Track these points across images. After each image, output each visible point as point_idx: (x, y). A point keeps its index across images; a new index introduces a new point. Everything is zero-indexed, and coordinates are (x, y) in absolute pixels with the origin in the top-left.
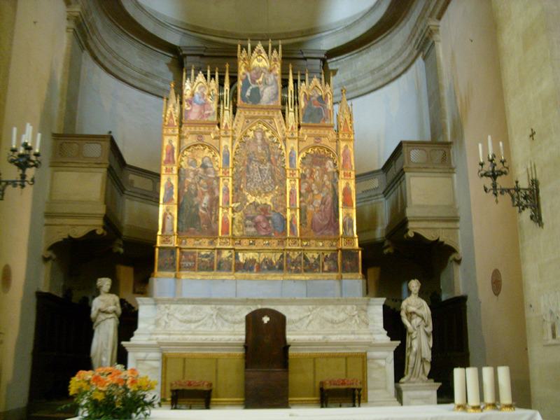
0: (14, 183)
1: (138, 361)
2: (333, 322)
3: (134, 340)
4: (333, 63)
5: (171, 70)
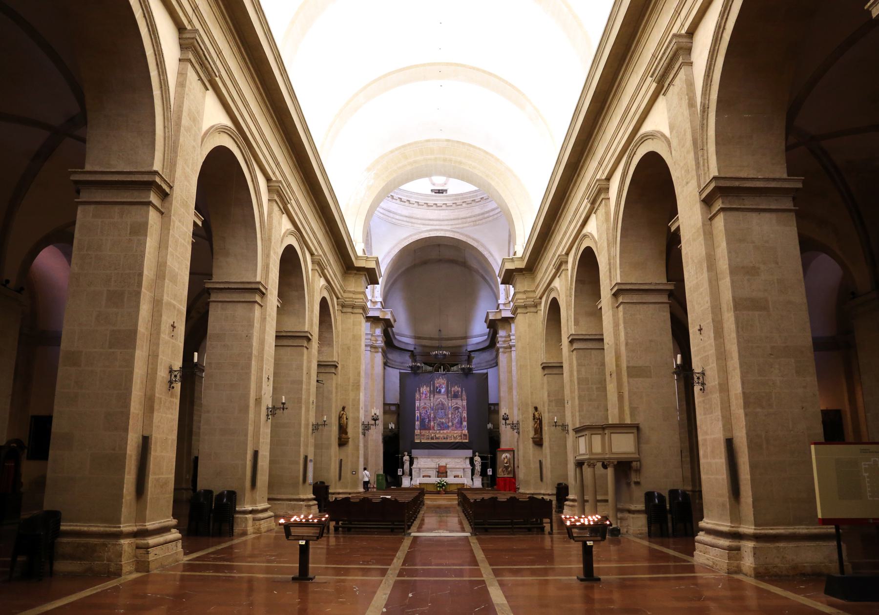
3: (413, 466)
4: (473, 355)
5: (411, 358)
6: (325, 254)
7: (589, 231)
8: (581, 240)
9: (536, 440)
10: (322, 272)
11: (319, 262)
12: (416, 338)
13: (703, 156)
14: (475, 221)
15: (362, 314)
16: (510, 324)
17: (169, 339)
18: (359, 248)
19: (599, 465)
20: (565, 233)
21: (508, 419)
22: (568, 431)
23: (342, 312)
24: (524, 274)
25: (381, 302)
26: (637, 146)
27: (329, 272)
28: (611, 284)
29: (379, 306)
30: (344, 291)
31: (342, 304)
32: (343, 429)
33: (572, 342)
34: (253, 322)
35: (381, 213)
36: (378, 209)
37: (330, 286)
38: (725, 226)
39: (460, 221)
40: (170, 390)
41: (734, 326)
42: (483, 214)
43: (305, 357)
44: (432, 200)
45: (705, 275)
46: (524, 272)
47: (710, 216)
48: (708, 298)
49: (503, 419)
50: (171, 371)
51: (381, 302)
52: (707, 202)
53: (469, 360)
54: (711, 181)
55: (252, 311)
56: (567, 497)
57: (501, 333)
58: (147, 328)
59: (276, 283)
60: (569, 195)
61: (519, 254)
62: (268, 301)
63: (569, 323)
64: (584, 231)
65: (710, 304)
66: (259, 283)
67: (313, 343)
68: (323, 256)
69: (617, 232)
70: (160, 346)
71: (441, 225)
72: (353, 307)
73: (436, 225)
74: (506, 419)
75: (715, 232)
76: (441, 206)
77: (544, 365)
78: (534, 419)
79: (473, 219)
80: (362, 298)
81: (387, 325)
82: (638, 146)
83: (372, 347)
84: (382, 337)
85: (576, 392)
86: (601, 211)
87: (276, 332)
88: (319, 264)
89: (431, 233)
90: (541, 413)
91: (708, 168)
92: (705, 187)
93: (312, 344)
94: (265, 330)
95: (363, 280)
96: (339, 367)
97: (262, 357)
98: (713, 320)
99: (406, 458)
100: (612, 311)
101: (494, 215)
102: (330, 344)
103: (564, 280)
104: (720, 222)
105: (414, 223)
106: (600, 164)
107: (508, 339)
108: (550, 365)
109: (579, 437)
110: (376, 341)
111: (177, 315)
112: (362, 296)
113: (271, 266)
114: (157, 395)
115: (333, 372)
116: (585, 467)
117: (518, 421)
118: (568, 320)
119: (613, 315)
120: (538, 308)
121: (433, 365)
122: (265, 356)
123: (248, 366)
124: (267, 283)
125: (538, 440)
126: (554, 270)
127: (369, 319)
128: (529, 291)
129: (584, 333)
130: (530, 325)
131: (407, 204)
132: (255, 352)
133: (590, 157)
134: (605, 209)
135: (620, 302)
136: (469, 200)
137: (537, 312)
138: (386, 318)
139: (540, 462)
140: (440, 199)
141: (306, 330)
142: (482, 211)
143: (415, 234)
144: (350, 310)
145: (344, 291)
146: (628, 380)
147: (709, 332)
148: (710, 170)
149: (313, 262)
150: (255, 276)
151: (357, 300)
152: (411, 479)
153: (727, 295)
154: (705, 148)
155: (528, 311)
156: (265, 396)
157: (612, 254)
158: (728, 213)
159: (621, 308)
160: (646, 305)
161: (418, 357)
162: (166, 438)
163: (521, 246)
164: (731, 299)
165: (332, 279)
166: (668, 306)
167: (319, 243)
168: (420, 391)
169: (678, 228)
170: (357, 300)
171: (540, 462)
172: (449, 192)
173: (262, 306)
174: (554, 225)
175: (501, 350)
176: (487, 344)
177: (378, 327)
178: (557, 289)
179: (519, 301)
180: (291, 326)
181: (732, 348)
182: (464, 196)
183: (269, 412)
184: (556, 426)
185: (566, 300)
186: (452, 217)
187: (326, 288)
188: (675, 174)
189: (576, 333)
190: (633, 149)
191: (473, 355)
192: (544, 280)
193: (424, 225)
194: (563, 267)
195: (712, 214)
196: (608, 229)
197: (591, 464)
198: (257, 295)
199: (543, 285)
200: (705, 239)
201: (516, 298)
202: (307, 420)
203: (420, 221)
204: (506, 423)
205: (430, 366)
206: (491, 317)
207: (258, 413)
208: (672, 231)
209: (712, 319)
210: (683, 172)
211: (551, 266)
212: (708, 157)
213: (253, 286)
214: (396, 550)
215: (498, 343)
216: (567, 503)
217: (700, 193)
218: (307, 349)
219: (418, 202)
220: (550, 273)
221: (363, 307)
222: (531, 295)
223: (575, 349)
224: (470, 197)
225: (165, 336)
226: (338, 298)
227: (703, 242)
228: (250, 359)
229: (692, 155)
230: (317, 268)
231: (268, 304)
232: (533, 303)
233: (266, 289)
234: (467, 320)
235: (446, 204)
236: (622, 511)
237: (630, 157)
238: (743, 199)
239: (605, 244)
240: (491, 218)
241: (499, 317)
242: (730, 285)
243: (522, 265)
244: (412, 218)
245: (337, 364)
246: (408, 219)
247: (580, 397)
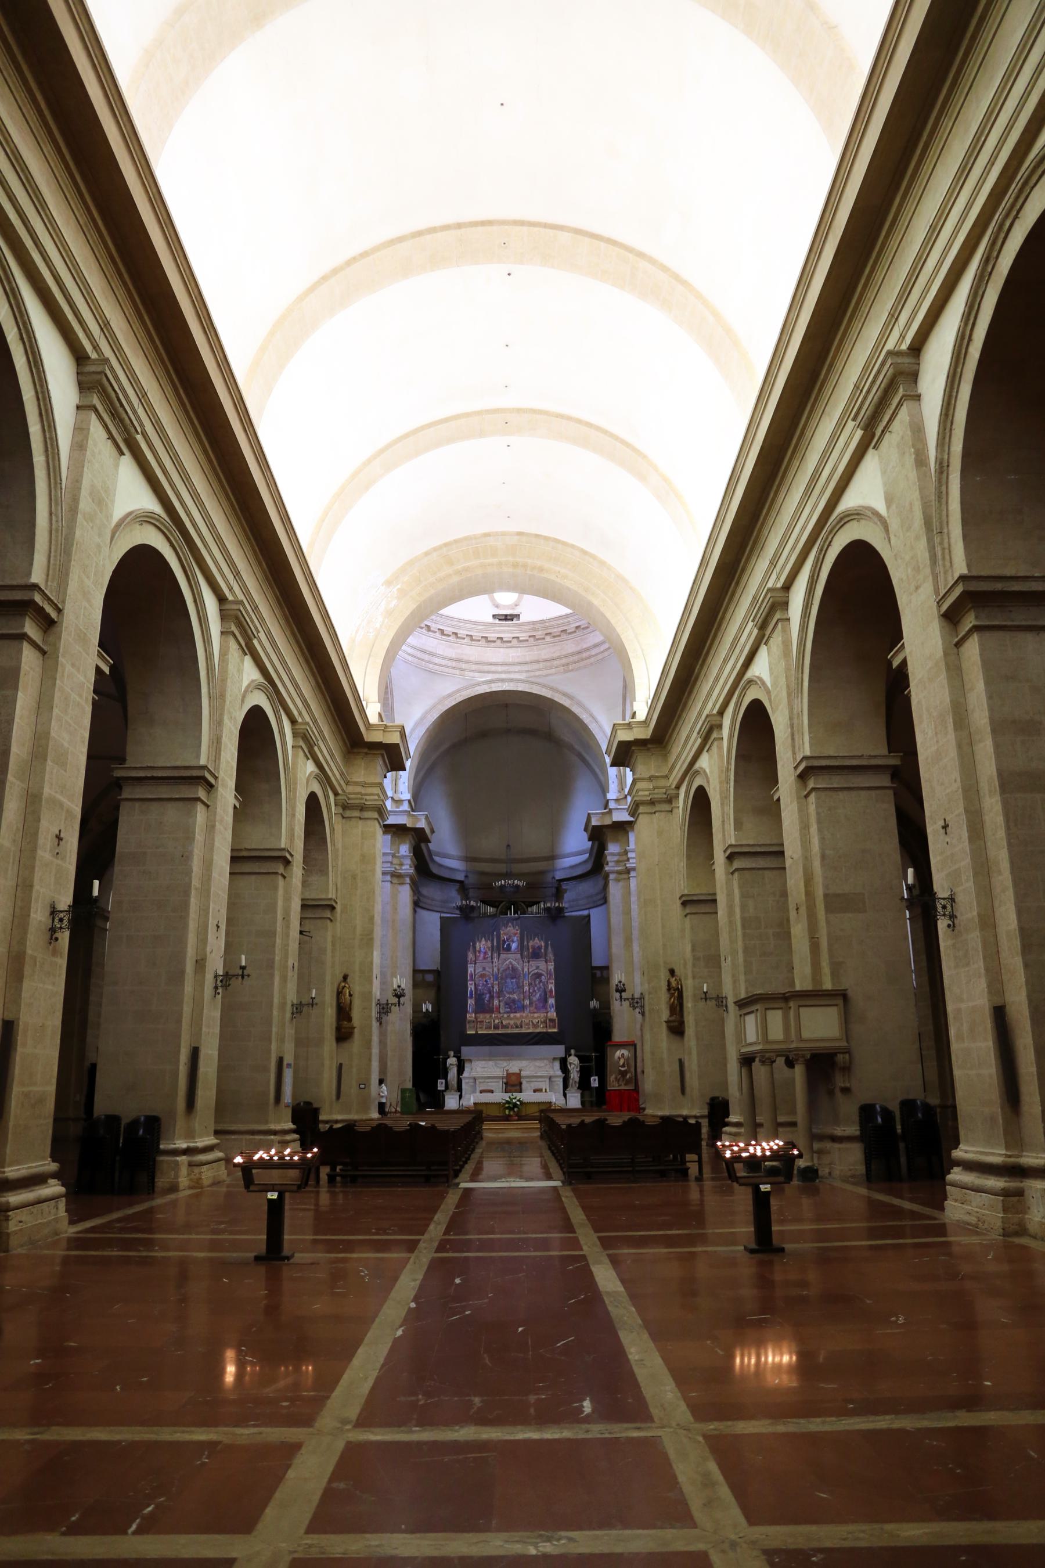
0: (395, 1005)
1: (466, 1083)
2: (539, 1067)
4: (564, 886)
6: (315, 721)
7: (757, 674)
8: (744, 688)
9: (672, 1024)
10: (309, 752)
11: (304, 734)
12: (468, 859)
13: (941, 543)
14: (567, 665)
15: (377, 819)
16: (627, 833)
17: (51, 858)
18: (373, 712)
19: (781, 1061)
20: (717, 679)
21: (624, 991)
22: (726, 1006)
23: (343, 818)
24: (648, 749)
25: (409, 801)
26: (834, 532)
27: (322, 752)
28: (794, 759)
29: (405, 807)
30: (347, 783)
31: (343, 804)
32: (343, 1012)
33: (730, 858)
34: (194, 833)
35: (409, 654)
36: (404, 647)
37: (323, 775)
38: (981, 655)
39: (541, 665)
40: (50, 943)
41: (1002, 818)
42: (579, 653)
43: (281, 892)
44: (495, 631)
45: (951, 736)
46: (649, 746)
47: (956, 640)
48: (956, 775)
49: (617, 991)
50: (54, 912)
51: (409, 801)
52: (951, 617)
53: (559, 894)
54: (956, 582)
55: (191, 814)
56: (726, 1120)
57: (613, 848)
58: (14, 841)
59: (232, 767)
60: (723, 618)
61: (641, 716)
62: (219, 797)
63: (726, 826)
64: (749, 675)
65: (960, 784)
66: (204, 767)
67: (294, 868)
68: (312, 725)
69: (802, 673)
70: (37, 869)
71: (509, 672)
72: (362, 808)
73: (501, 673)
74: (621, 990)
75: (964, 666)
76: (510, 642)
77: (684, 899)
78: (669, 989)
79: (564, 661)
80: (376, 792)
81: (419, 838)
82: (834, 531)
83: (395, 875)
84: (411, 859)
85: (740, 943)
86: (776, 640)
87: (232, 850)
88: (302, 736)
89: (493, 685)
90: (680, 980)
91: (951, 563)
92: (946, 593)
93: (292, 870)
94: (213, 844)
95: (379, 764)
96: (338, 907)
97: (208, 891)
98: (966, 811)
99: (452, 1061)
100: (798, 803)
101: (596, 655)
102: (324, 871)
103: (716, 756)
104: (973, 648)
105: (465, 670)
106: (773, 563)
107: (625, 858)
108: (695, 898)
109: (745, 1014)
110: (401, 864)
111: (66, 819)
112: (376, 790)
113: (225, 739)
114: (29, 951)
115: (329, 916)
116: (756, 1065)
117: (641, 994)
118: (723, 821)
119: (800, 810)
120: (674, 805)
121: (497, 904)
122: (212, 889)
123: (186, 905)
124: (217, 768)
125: (676, 1024)
126: (699, 741)
127: (388, 828)
128: (657, 777)
129: (751, 842)
130: (660, 833)
131: (452, 638)
132: (195, 883)
133: (756, 553)
134: (782, 637)
135: (811, 787)
136: (555, 630)
137: (671, 811)
138: (417, 826)
139: (681, 1062)
140: (507, 630)
141: (283, 846)
142: (578, 648)
143: (466, 688)
144: (356, 813)
145: (347, 783)
146: (827, 919)
147: (961, 832)
148: (955, 566)
149: (295, 735)
150: (198, 757)
151: (365, 797)
152: (461, 1097)
153: (987, 768)
154: (945, 531)
155: (657, 809)
156: (213, 955)
157: (795, 711)
158: (987, 634)
159: (812, 798)
160: (854, 793)
161: (471, 890)
162: (43, 1026)
163: (642, 705)
164: (995, 773)
165: (327, 762)
166: (891, 792)
167: (305, 702)
168: (474, 947)
169: (904, 663)
170: (368, 798)
171: (681, 1062)
172: (522, 619)
173: (208, 806)
174: (698, 667)
175: (612, 877)
176: (588, 867)
177: (404, 842)
178: (705, 772)
179: (641, 793)
180: (257, 839)
181: (1001, 855)
182: (548, 624)
183: (218, 982)
184: (706, 999)
185: (720, 788)
186: (528, 659)
187: (317, 777)
188: (897, 575)
189: (739, 843)
190: (827, 538)
191: (564, 886)
192: (683, 757)
193: (480, 672)
194: (715, 735)
195: (959, 637)
196: (787, 669)
197: (766, 1059)
198: (200, 787)
199: (681, 766)
200: (950, 679)
201: (637, 787)
202: (284, 997)
203: (474, 667)
204: (621, 997)
205: (492, 906)
206: (594, 822)
207: (200, 984)
208: (894, 667)
209: (965, 808)
210: (910, 570)
211: (695, 734)
212: (949, 545)
213: (195, 773)
214: (434, 1210)
215: (607, 864)
216: (726, 1129)
217: (938, 603)
218: (284, 877)
219: (471, 636)
220: (693, 745)
221: (379, 808)
222: (662, 783)
223: (736, 870)
224: (558, 626)
225: (44, 853)
226: (336, 794)
227: (945, 682)
228: (187, 894)
229: (923, 542)
230: (302, 743)
231: (218, 803)
232: (665, 796)
233: (216, 778)
234: (555, 826)
235: (518, 638)
236: (821, 1138)
237: (821, 550)
238: (1011, 611)
239: (784, 694)
240: (592, 660)
241: (607, 821)
242: (992, 750)
243: (646, 734)
244: (460, 661)
245: (334, 904)
246: (454, 664)
247: (746, 950)
